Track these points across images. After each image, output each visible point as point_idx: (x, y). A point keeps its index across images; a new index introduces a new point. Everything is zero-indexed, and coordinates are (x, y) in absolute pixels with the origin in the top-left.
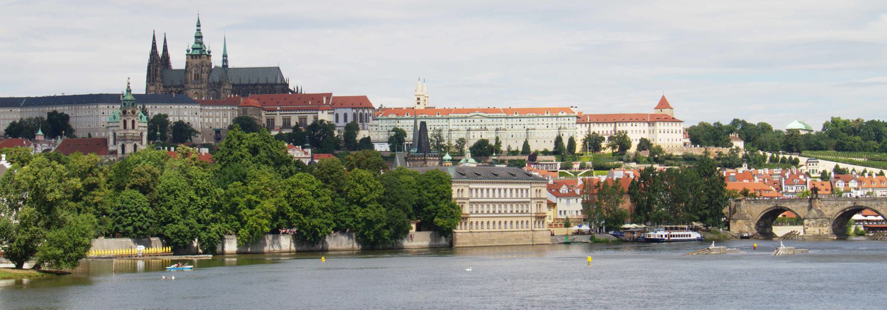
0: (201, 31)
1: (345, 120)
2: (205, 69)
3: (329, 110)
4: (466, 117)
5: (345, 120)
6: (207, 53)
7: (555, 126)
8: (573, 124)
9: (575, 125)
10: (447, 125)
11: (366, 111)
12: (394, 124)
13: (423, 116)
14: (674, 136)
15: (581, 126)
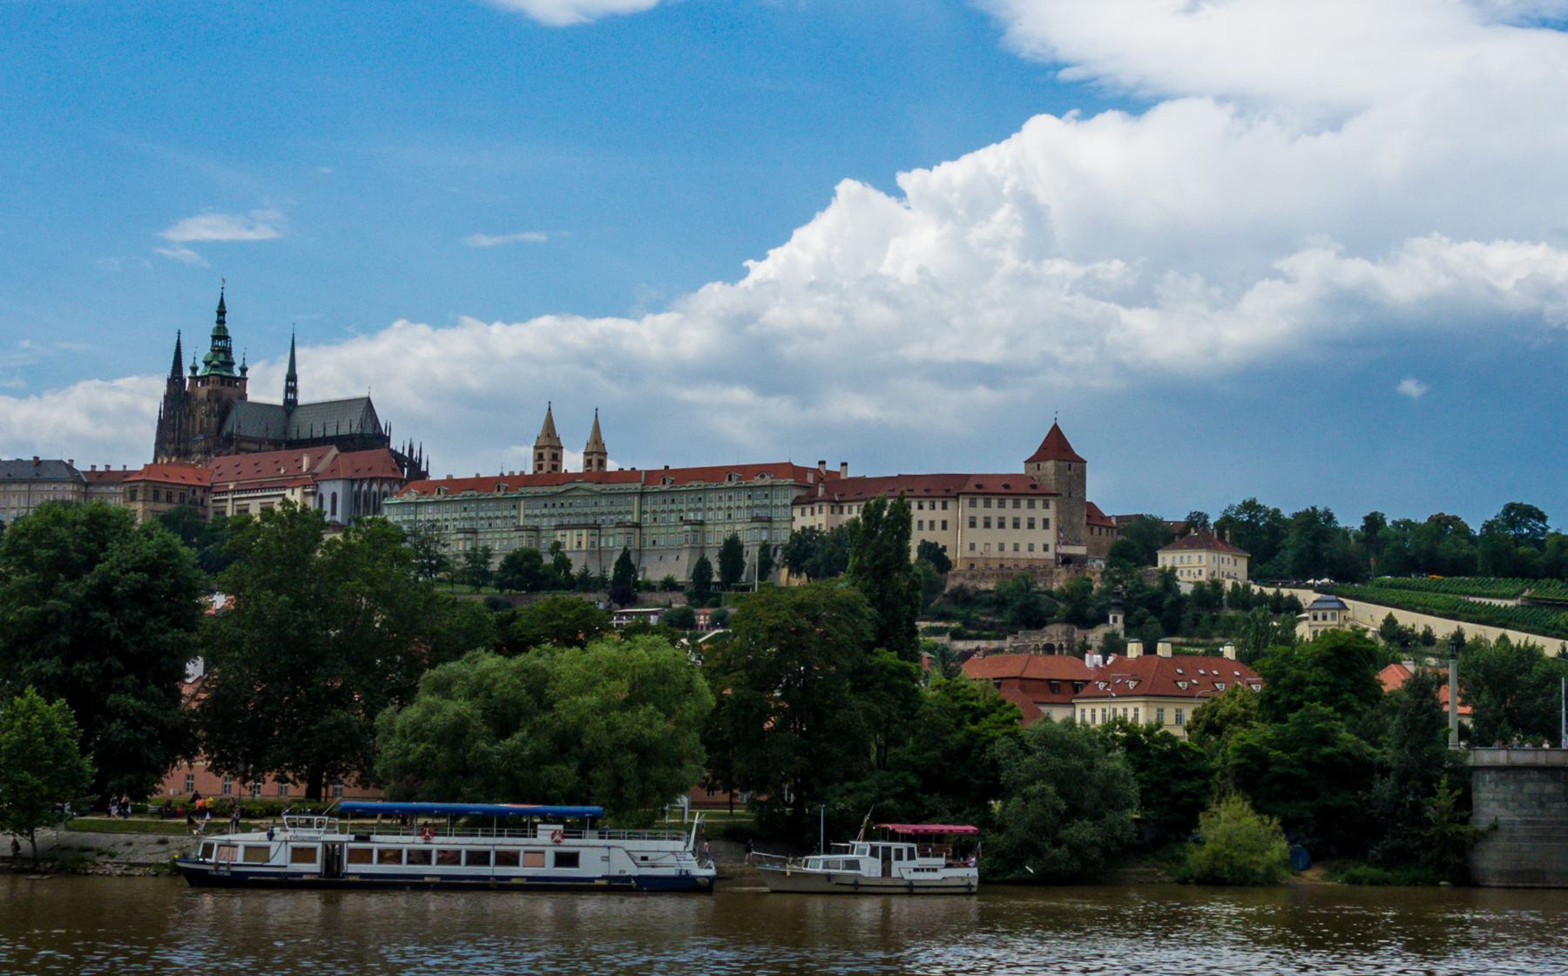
0: (226, 325)
1: (334, 513)
2: (212, 410)
3: (305, 487)
4: (555, 495)
5: (334, 513)
6: (238, 373)
7: (744, 514)
8: (785, 506)
9: (789, 509)
10: (513, 517)
11: (375, 487)
12: (412, 517)
13: (469, 493)
14: (1023, 537)
15: (803, 514)
